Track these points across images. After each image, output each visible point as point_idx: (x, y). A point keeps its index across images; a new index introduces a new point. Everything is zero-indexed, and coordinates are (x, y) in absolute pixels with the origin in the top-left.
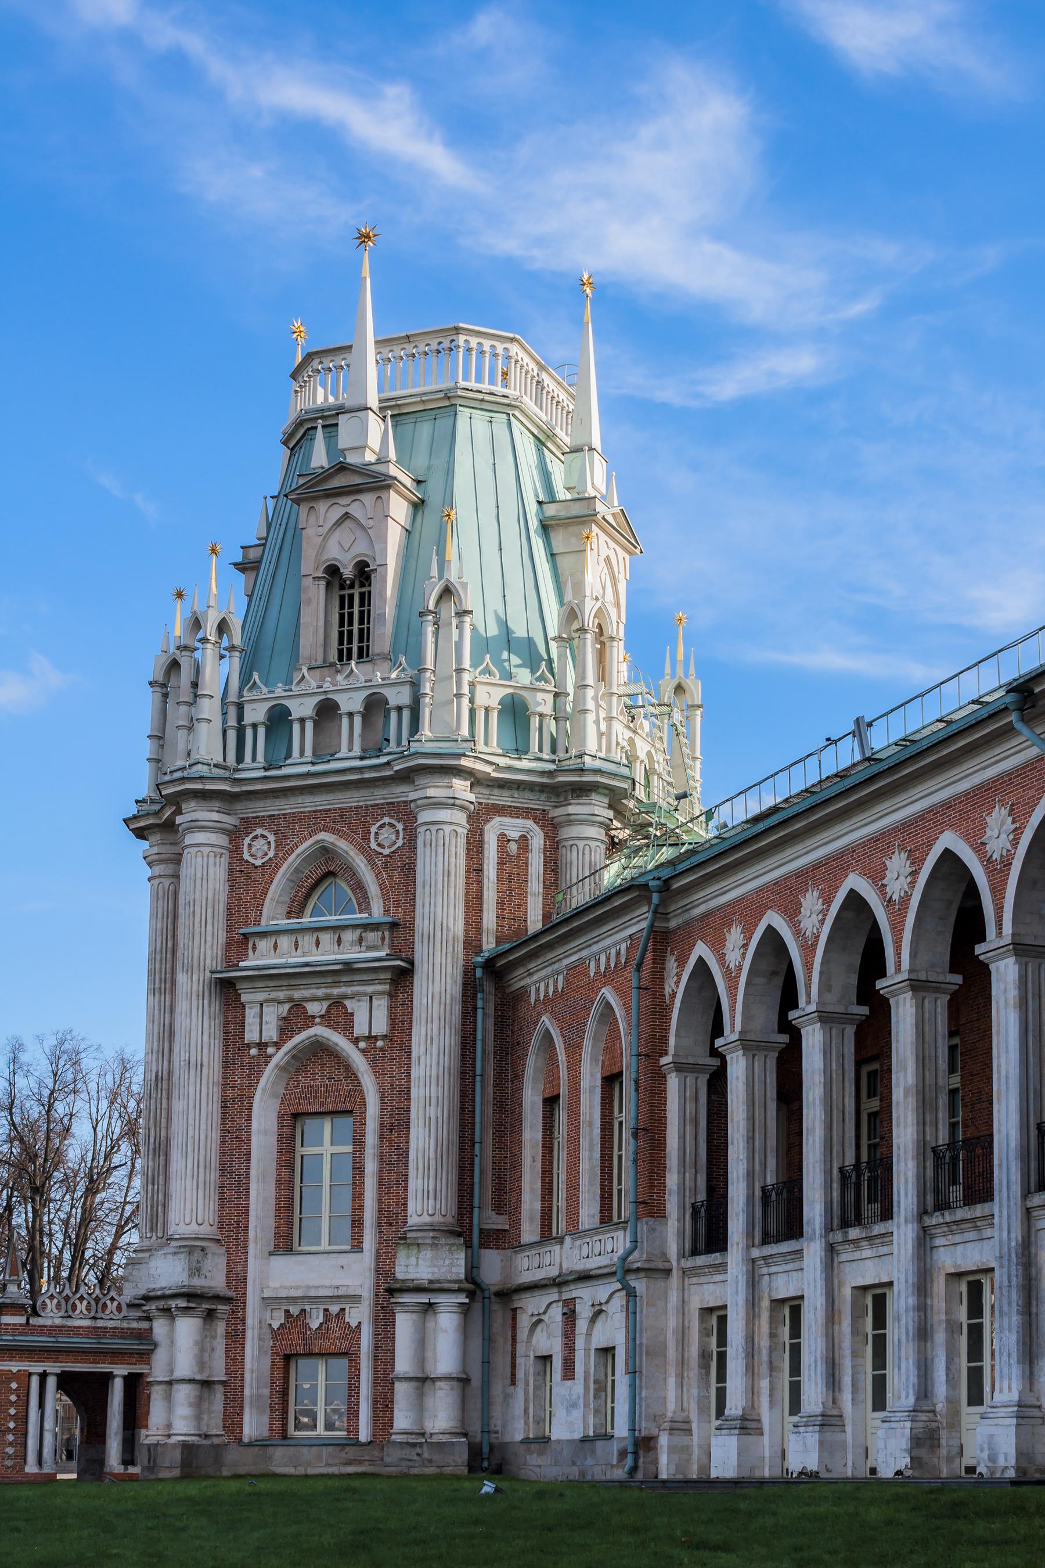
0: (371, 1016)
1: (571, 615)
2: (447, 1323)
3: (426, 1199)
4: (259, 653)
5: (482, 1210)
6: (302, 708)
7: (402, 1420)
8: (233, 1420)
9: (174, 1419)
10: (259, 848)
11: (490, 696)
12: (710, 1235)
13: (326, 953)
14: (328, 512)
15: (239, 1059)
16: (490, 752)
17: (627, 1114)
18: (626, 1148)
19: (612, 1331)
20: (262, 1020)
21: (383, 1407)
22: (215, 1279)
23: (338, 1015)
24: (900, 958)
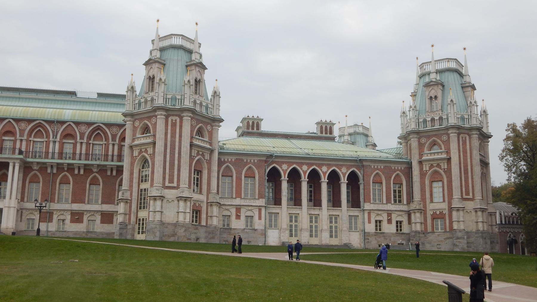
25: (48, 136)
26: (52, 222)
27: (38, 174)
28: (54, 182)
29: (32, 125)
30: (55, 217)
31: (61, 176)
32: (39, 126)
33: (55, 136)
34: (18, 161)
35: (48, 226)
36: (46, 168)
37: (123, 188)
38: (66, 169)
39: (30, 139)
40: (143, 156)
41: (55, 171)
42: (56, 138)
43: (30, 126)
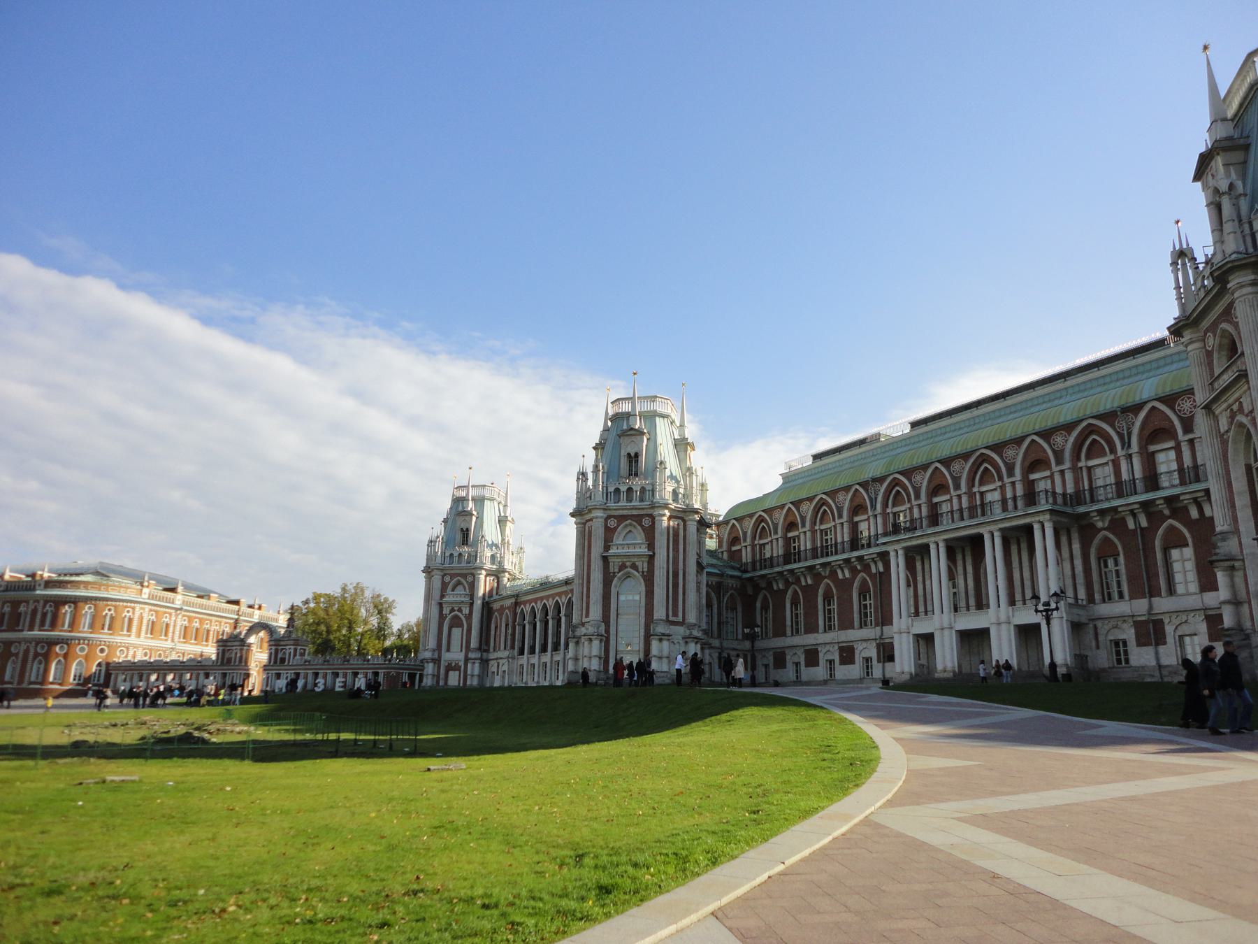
0: (466, 611)
1: (503, 540)
2: (477, 665)
3: (474, 643)
4: (447, 542)
5: (484, 645)
6: (456, 554)
7: (468, 682)
8: (438, 682)
9: (428, 681)
10: (447, 579)
11: (489, 554)
12: (522, 652)
13: (459, 599)
14: (462, 518)
15: (442, 617)
16: (488, 566)
17: (510, 631)
18: (509, 637)
19: (505, 668)
20: (446, 611)
21: (465, 680)
22: (436, 656)
23: (460, 610)
24: (550, 613)
25: (1113, 450)
26: (1165, 643)
27: (1111, 536)
28: (1148, 549)
29: (1075, 433)
30: (1169, 629)
31: (1160, 532)
32: (1091, 432)
33: (1126, 444)
34: (1047, 516)
35: (1157, 653)
36: (1123, 520)
37: (1218, 529)
38: (1167, 512)
39: (1080, 465)
40: (1241, 425)
41: (1144, 523)
42: (1129, 446)
43: (1071, 439)
